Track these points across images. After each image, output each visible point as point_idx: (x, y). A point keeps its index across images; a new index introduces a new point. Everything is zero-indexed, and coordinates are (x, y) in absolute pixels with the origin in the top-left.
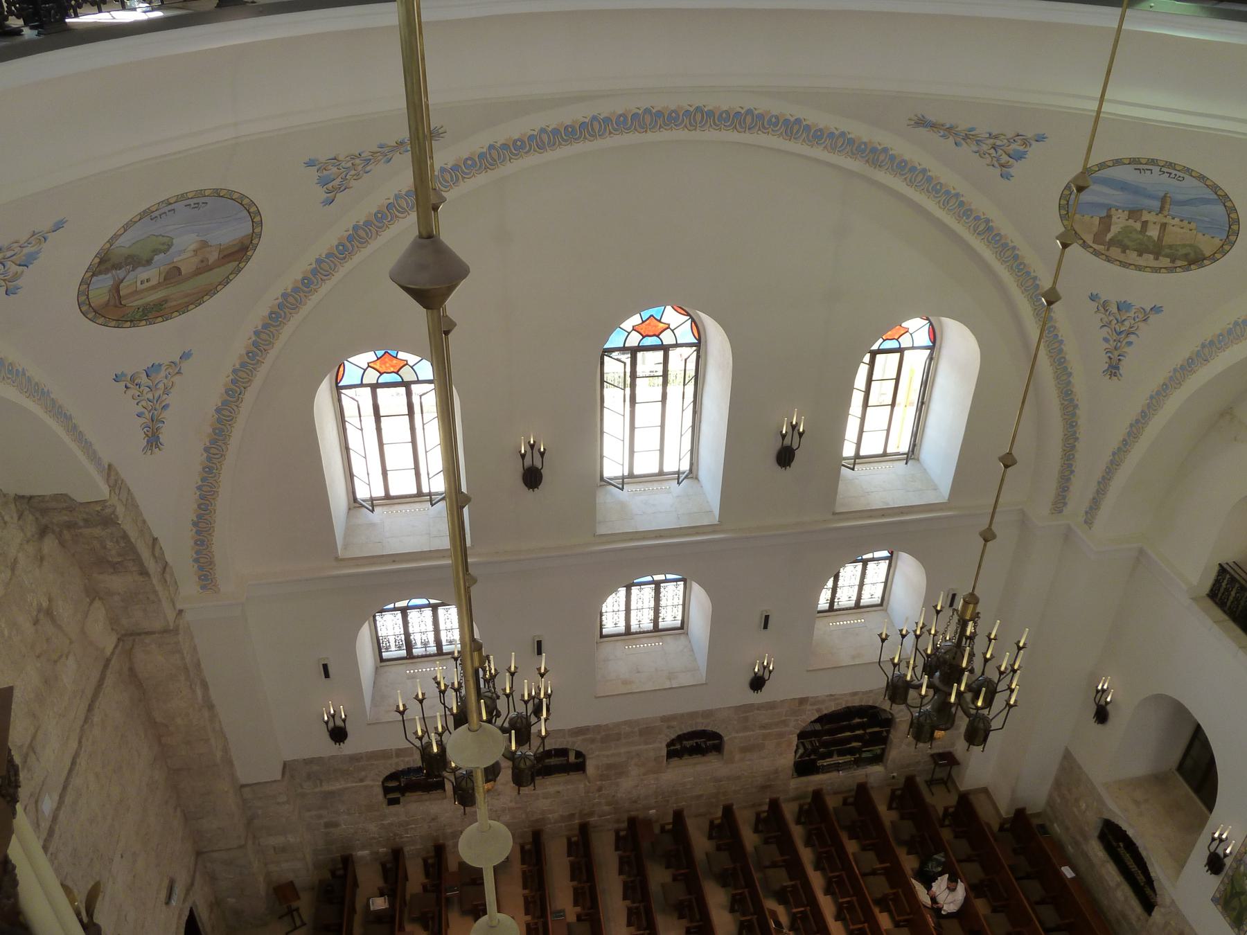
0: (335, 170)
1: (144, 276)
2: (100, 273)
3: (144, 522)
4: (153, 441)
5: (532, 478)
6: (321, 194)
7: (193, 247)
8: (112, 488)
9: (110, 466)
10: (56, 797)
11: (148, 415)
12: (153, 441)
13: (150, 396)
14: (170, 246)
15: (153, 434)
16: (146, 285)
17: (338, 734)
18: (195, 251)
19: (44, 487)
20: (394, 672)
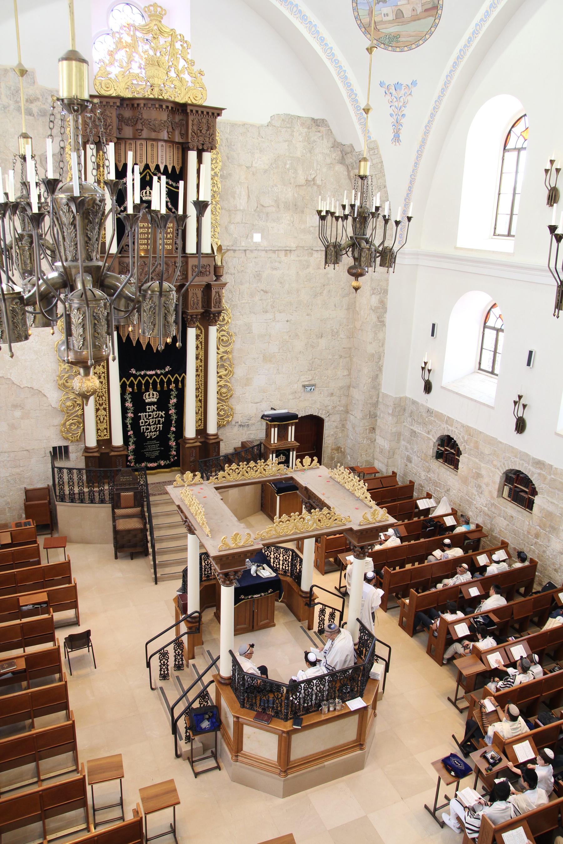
4: (397, 138)
8: (370, 149)
9: (375, 141)
10: (265, 244)
11: (395, 118)
12: (397, 138)
13: (396, 104)
15: (397, 132)
16: (385, 19)
17: (428, 388)
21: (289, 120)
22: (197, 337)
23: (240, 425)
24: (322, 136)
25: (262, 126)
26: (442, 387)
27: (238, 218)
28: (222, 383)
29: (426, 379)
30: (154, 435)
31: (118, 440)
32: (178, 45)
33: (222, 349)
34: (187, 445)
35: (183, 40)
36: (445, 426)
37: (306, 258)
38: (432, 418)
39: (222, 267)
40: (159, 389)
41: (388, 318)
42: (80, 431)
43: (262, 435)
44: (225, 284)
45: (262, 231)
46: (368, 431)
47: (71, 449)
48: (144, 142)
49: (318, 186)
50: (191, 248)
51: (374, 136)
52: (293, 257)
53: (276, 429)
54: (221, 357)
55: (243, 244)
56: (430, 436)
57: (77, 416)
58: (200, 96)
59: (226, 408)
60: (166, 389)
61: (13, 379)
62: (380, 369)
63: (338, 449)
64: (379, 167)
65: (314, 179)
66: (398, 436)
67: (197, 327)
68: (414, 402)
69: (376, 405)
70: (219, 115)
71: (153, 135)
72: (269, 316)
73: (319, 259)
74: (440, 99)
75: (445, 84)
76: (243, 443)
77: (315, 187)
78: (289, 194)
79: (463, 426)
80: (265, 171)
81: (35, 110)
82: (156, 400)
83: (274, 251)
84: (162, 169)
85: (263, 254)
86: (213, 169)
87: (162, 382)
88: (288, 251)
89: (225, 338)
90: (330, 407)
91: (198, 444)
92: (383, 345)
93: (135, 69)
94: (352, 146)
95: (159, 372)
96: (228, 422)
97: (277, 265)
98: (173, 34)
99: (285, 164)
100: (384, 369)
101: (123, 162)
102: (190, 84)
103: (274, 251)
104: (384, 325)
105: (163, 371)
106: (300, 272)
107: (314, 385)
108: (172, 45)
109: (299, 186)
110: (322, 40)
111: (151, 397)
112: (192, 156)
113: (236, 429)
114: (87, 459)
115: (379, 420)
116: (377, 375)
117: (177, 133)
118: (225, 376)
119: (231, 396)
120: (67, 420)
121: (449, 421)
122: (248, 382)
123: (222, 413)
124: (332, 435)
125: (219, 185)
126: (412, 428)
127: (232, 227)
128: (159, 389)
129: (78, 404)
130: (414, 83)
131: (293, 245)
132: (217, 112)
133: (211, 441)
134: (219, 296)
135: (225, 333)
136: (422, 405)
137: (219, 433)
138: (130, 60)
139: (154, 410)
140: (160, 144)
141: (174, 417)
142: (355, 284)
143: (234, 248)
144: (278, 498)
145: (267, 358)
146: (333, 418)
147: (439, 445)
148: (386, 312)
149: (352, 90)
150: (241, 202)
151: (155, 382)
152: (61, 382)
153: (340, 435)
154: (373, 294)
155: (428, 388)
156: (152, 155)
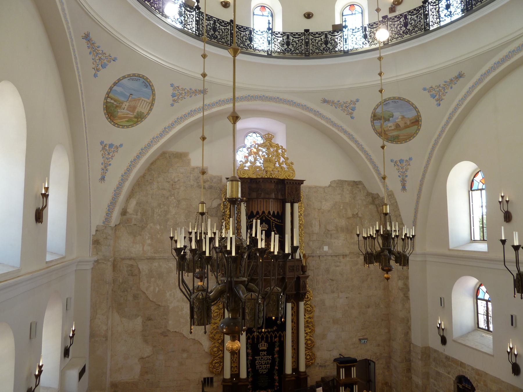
0: (434, 92)
1: (389, 125)
2: (375, 120)
3: (400, 216)
4: (404, 188)
5: (508, 217)
6: (434, 102)
7: (400, 117)
8: (389, 195)
9: (391, 191)
10: (331, 252)
12: (404, 188)
13: (401, 170)
14: (393, 115)
17: (444, 341)
18: (402, 119)
19: (375, 192)
20: (479, 333)
21: (340, 183)
22: (292, 308)
23: (320, 366)
24: (360, 190)
25: (326, 187)
26: (453, 341)
27: (315, 237)
28: (308, 337)
29: (442, 334)
30: (265, 371)
31: (243, 375)
32: (280, 151)
33: (307, 316)
34: (287, 379)
35: (282, 148)
36: (460, 368)
37: (356, 259)
38: (450, 363)
39: (306, 266)
40: (269, 341)
41: (412, 294)
42: (221, 367)
43: (335, 373)
44: (308, 277)
45: (328, 244)
47: (214, 379)
48: (262, 200)
49: (360, 218)
51: (390, 188)
52: (348, 259)
53: (344, 369)
54: (307, 321)
55: (318, 252)
56: (450, 376)
57: (219, 358)
58: (291, 175)
59: (311, 354)
61: (184, 333)
62: (409, 328)
63: (386, 384)
64: (395, 206)
65: (357, 214)
66: (427, 376)
67: (292, 303)
68: (435, 351)
69: (409, 352)
70: (302, 183)
71: (267, 196)
72: (335, 295)
74: (426, 167)
75: (429, 158)
76: (322, 378)
77: (358, 218)
78: (343, 223)
79: (473, 369)
80: (329, 211)
81: (207, 186)
82: (266, 348)
83: (336, 256)
84: (272, 213)
85: (330, 258)
86: (299, 212)
87: (271, 336)
88: (345, 256)
89: (309, 309)
90: (378, 354)
91: (293, 378)
92: (409, 312)
93: (258, 164)
94: (378, 194)
95: (269, 330)
96: (312, 363)
97: (338, 263)
98: (277, 146)
99: (340, 207)
100: (412, 328)
101: (251, 210)
102: (286, 169)
103: (336, 256)
104: (409, 299)
105: (272, 330)
108: (277, 151)
109: (349, 218)
110: (356, 142)
111: (263, 346)
112: (288, 205)
113: (317, 368)
114: (224, 387)
115: (412, 364)
117: (280, 194)
118: (310, 332)
119: (314, 346)
120: (214, 360)
121: (462, 364)
122: (324, 337)
123: (308, 357)
125: (303, 221)
126: (436, 369)
127: (311, 243)
128: (269, 341)
129: (221, 350)
130: (410, 159)
131: (347, 252)
132: (302, 182)
133: (302, 377)
134: (305, 283)
135: (309, 306)
136: (442, 353)
137: (307, 371)
138: (256, 160)
139: (265, 355)
140: (270, 200)
141: (277, 360)
142: (386, 276)
143: (313, 255)
145: (335, 322)
147: (457, 383)
148: (409, 290)
149: (375, 165)
150: (316, 229)
151: (267, 337)
152: (211, 336)
153: (387, 373)
154: (399, 279)
155: (444, 341)
156: (266, 206)
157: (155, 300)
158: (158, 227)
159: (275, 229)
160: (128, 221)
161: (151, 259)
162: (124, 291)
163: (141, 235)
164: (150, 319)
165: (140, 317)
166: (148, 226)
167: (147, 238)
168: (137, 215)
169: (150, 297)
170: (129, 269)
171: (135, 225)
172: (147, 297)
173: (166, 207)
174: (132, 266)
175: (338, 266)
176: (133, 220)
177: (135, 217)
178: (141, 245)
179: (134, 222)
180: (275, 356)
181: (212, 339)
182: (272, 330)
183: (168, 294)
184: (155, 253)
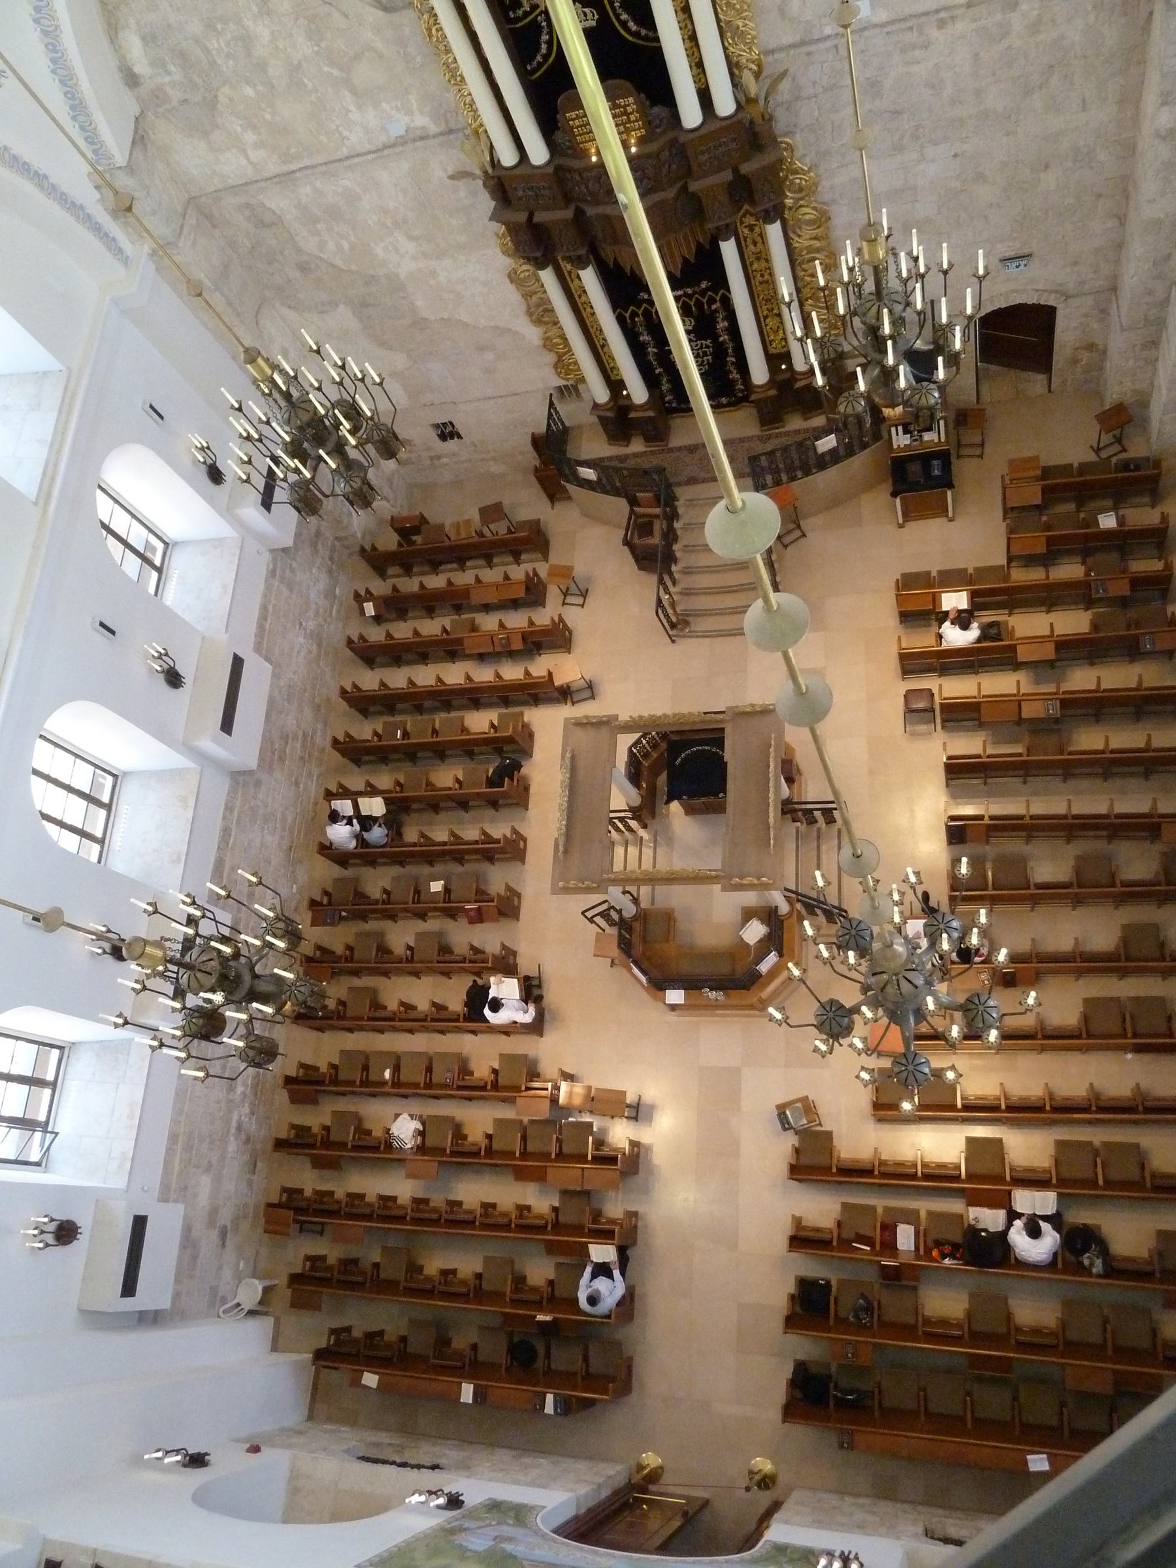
10: (883, 16)
31: (637, 391)
37: (999, 17)
46: (1138, 348)
50: (691, 115)
52: (960, 26)
60: (707, 312)
63: (1091, 347)
73: (1035, 13)
87: (699, 304)
91: (773, 392)
95: (689, 291)
106: (982, 54)
107: (1030, 255)
116: (1170, 254)
124: (1075, 328)
144: (898, 500)
146: (1074, 303)
154: (1165, 103)
157: (354, 268)
158: (249, 91)
159: (624, 17)
160: (159, 95)
161: (285, 178)
162: (270, 263)
163: (217, 126)
164: (367, 306)
165: (341, 307)
166: (221, 98)
167: (239, 129)
168: (169, 73)
169: (340, 263)
170: (247, 213)
171: (185, 101)
172: (332, 265)
173: (232, 26)
174: (248, 205)
175: (918, 62)
176: (168, 89)
177: (167, 79)
178: (235, 151)
179: (175, 95)
180: (721, 339)
181: (538, 322)
182: (696, 289)
183: (379, 251)
184: (285, 162)
